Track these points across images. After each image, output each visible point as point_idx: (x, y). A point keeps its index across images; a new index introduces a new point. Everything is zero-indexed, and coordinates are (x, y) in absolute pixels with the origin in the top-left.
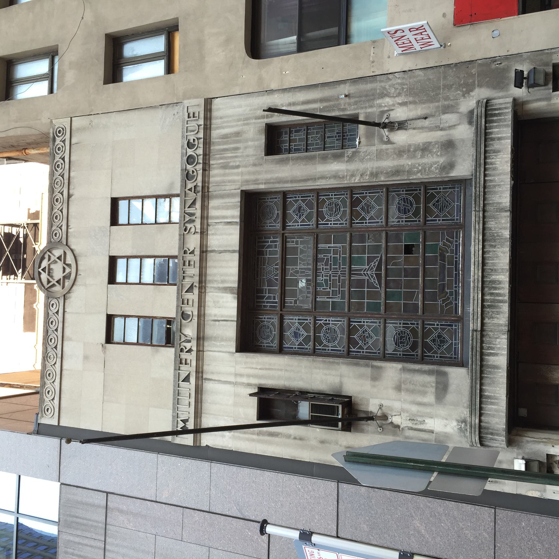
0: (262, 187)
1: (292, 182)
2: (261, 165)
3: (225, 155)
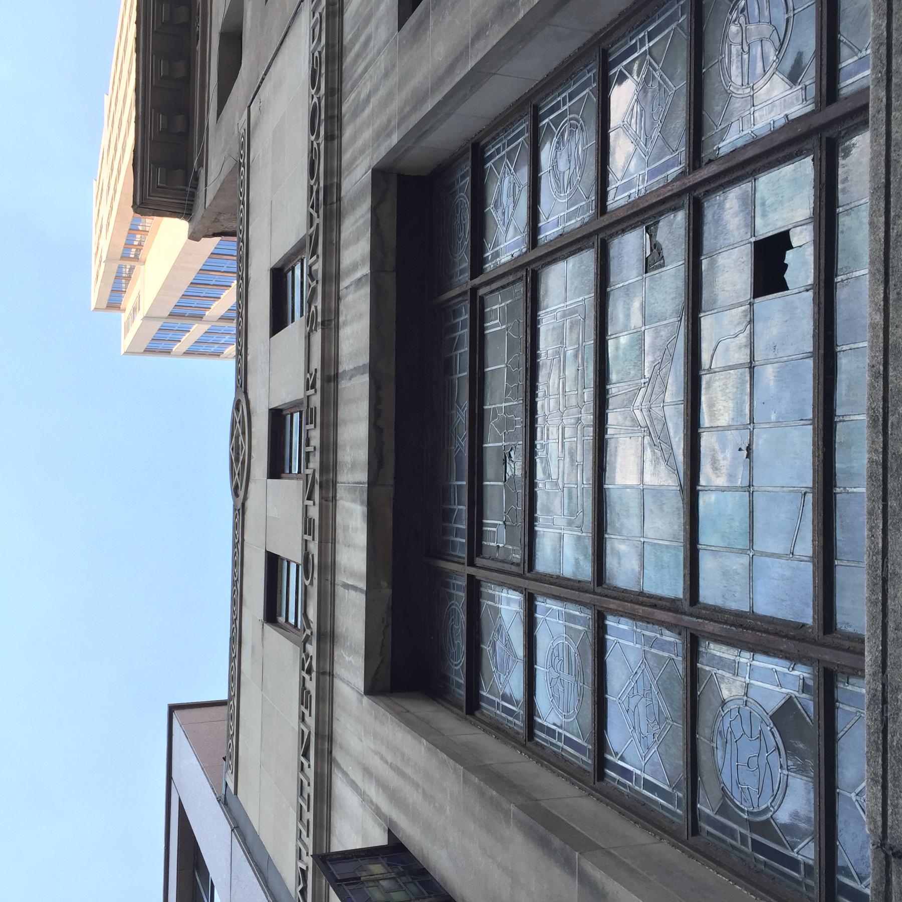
0: (395, 139)
1: (435, 87)
2: (394, 66)
3: (356, 75)
